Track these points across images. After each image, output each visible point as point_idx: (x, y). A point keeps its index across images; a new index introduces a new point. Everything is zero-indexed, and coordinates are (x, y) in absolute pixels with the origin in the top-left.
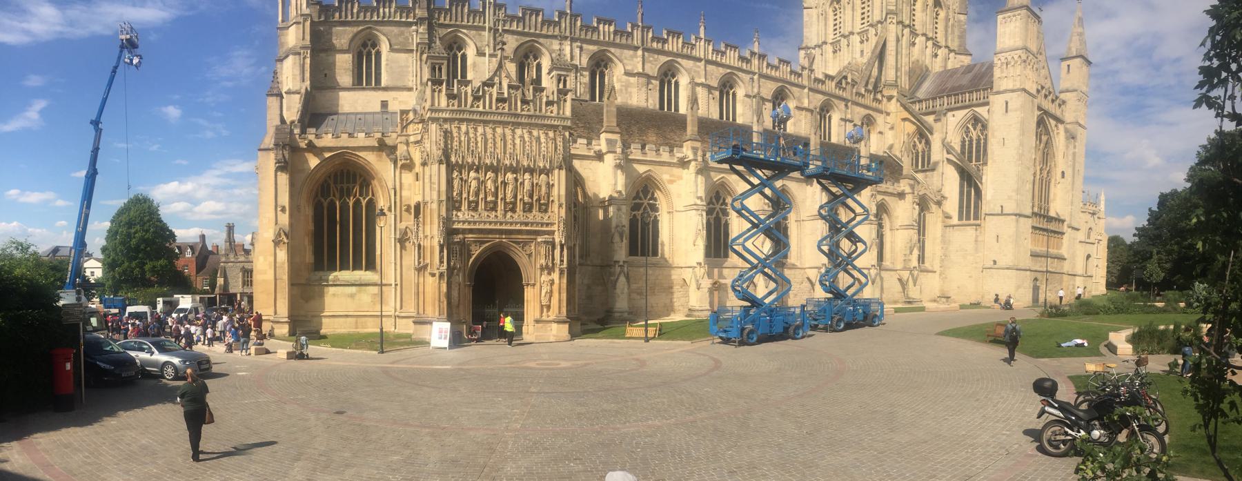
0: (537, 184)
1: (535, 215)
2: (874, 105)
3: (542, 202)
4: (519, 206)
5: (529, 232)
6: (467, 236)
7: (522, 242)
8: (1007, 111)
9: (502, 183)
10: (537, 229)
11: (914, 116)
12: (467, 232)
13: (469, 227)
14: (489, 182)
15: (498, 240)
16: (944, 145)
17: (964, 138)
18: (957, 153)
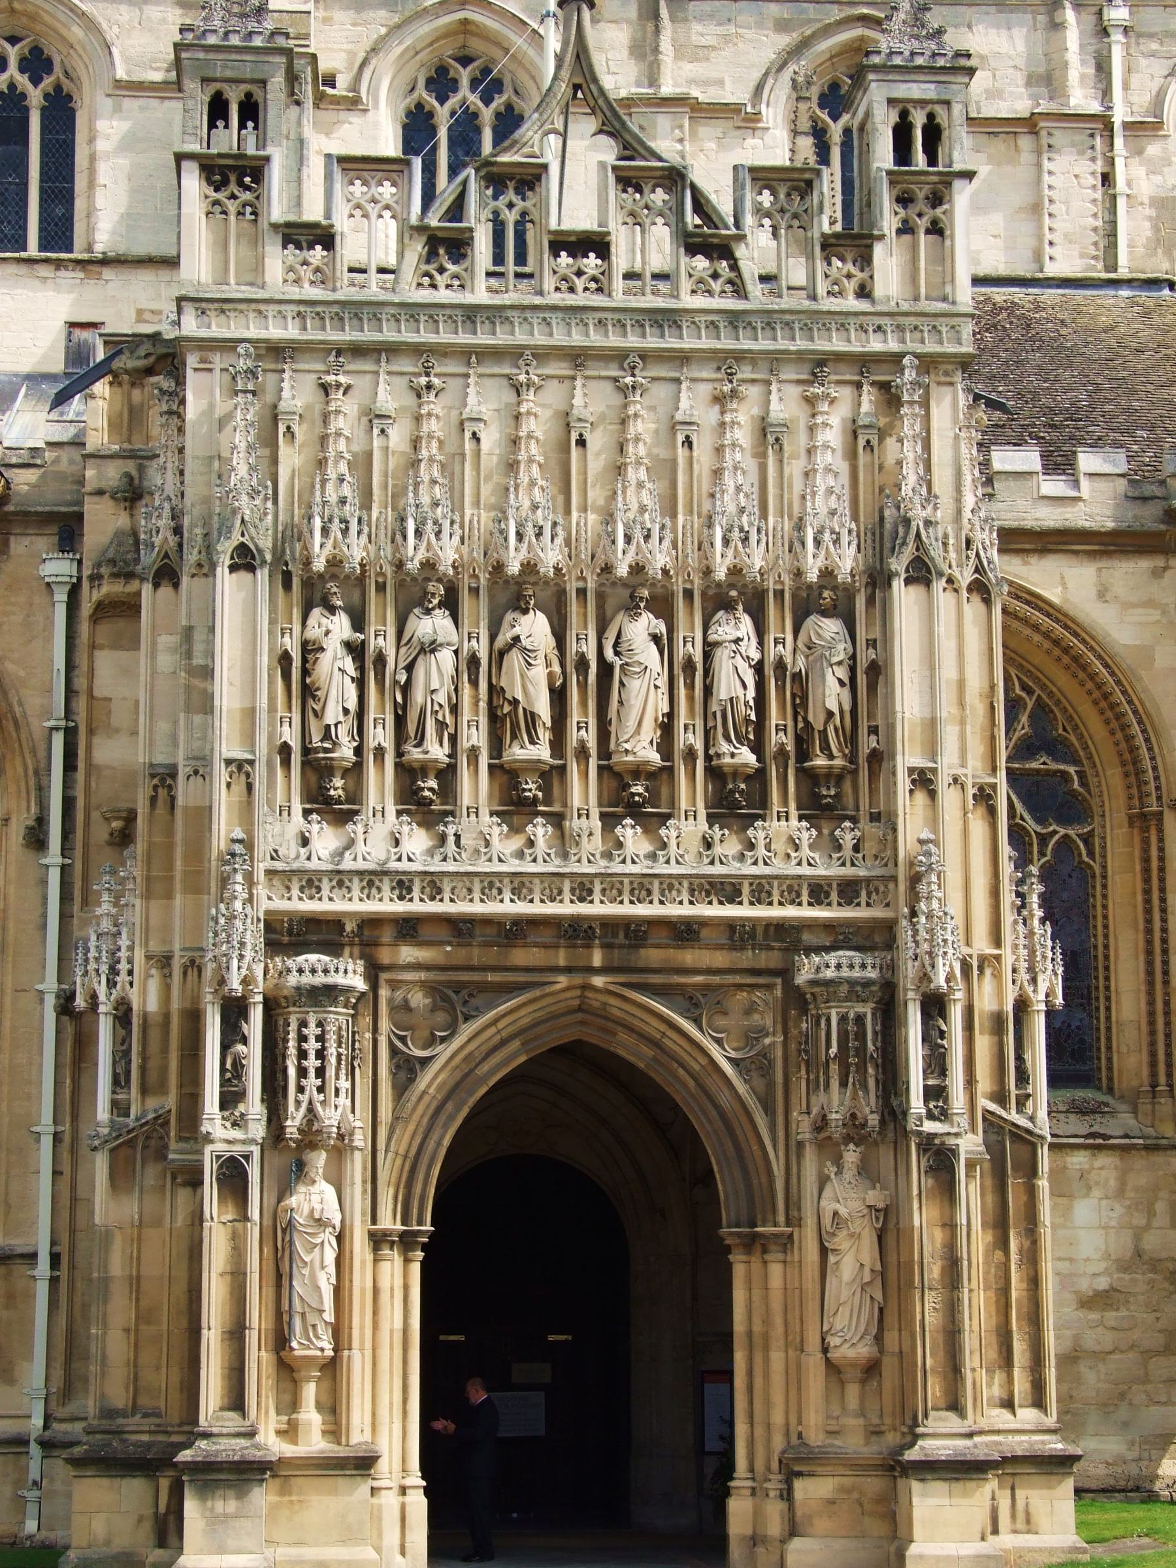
7: (706, 988)
10: (791, 912)
13: (400, 907)
14: (514, 659)
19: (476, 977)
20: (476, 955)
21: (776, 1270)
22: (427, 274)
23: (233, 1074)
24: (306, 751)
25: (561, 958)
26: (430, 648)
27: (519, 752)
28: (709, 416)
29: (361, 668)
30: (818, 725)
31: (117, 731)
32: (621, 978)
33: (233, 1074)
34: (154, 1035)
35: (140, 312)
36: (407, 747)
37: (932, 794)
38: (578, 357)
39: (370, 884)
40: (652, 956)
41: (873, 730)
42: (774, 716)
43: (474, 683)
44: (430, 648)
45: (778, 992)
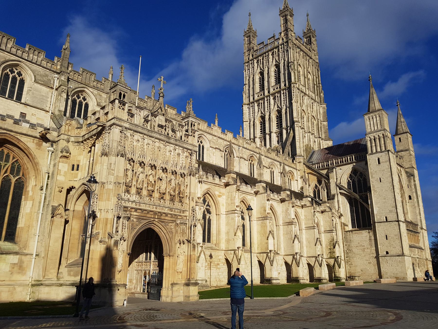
0: (178, 183)
1: (177, 205)
2: (293, 165)
3: (181, 196)
4: (167, 197)
7: (167, 222)
8: (379, 163)
9: (158, 178)
10: (178, 214)
11: (315, 171)
12: (133, 210)
13: (136, 207)
14: (151, 176)
15: (152, 219)
16: (337, 185)
17: (349, 181)
18: (346, 189)
20: (143, 215)
21: (171, 259)
23: (117, 228)
24: (125, 183)
27: (150, 188)
32: (159, 220)
36: (138, 185)
37: (193, 201)
38: (159, 139)
40: (162, 217)
41: (186, 193)
42: (176, 190)
43: (146, 178)
45: (175, 224)
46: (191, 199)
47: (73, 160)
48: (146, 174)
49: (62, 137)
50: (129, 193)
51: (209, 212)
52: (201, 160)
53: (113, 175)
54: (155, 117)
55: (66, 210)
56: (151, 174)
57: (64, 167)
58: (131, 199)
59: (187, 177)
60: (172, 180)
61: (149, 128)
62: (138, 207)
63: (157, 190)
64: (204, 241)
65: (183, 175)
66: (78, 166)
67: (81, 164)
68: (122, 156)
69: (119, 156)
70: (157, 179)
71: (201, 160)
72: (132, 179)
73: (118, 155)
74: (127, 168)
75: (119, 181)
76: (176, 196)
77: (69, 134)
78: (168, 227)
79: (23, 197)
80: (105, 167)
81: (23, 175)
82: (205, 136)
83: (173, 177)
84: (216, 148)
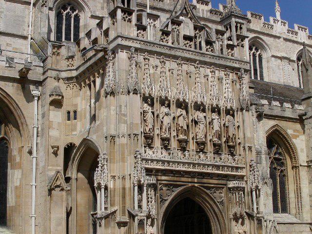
0: (224, 125)
1: (226, 158)
5: (219, 176)
6: (159, 178)
7: (213, 187)
9: (192, 120)
13: (163, 168)
14: (181, 118)
15: (190, 185)
19: (175, 183)
20: (175, 179)
22: (162, 39)
23: (140, 201)
24: (144, 133)
25: (190, 180)
26: (167, 114)
27: (181, 137)
28: (210, 75)
29: (154, 117)
30: (231, 137)
31: (54, 128)
32: (199, 185)
33: (140, 201)
34: (112, 192)
35: (7, 44)
39: (152, 162)
41: (239, 138)
42: (223, 135)
43: (174, 123)
44: (167, 114)
46: (247, 149)
47: (67, 106)
48: (173, 115)
49: (49, 73)
50: (151, 148)
51: (282, 164)
52: (259, 79)
53: (125, 122)
54: (179, 26)
55: (68, 180)
56: (180, 116)
57: (57, 116)
58: (154, 157)
59: (237, 114)
60: (214, 121)
61: (170, 44)
62: (166, 167)
63: (193, 139)
64: (276, 210)
65: (230, 112)
66: (75, 112)
67: (79, 110)
68: (135, 92)
69: (131, 94)
70: (190, 121)
71: (259, 79)
72: (154, 126)
73: (129, 92)
74: (144, 109)
75: (135, 132)
76: (224, 145)
77: (58, 68)
78: (215, 194)
79: (9, 164)
80: (113, 113)
81: (5, 133)
82: (263, 41)
83: (215, 116)
84: (281, 58)
